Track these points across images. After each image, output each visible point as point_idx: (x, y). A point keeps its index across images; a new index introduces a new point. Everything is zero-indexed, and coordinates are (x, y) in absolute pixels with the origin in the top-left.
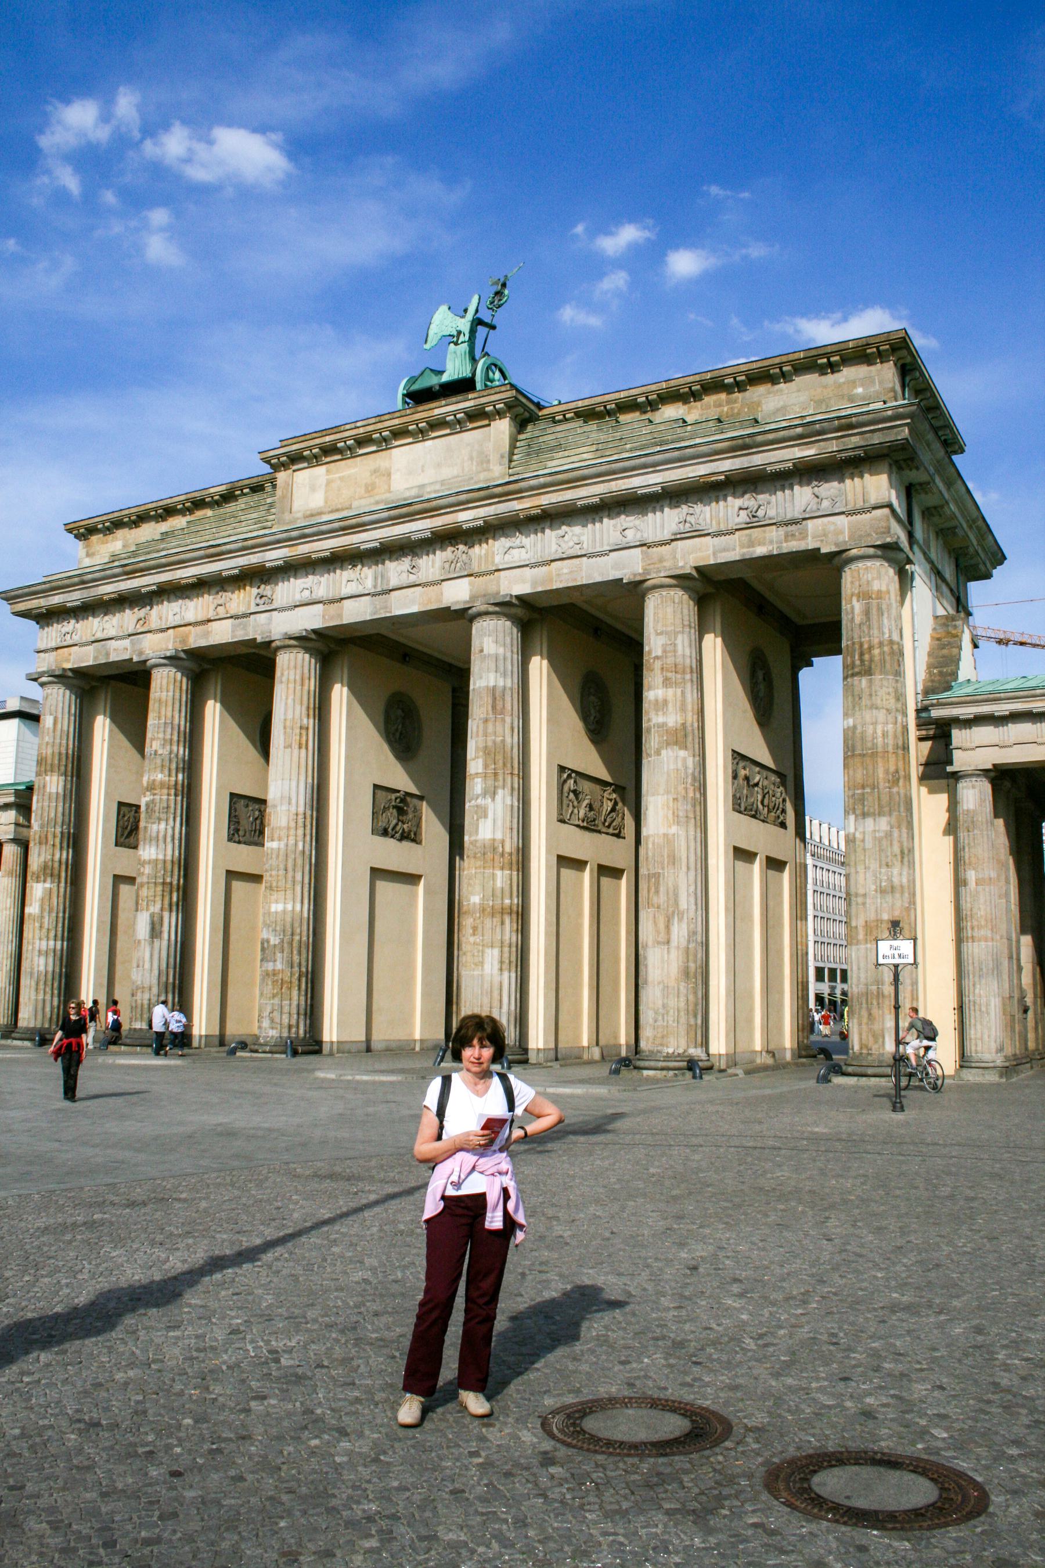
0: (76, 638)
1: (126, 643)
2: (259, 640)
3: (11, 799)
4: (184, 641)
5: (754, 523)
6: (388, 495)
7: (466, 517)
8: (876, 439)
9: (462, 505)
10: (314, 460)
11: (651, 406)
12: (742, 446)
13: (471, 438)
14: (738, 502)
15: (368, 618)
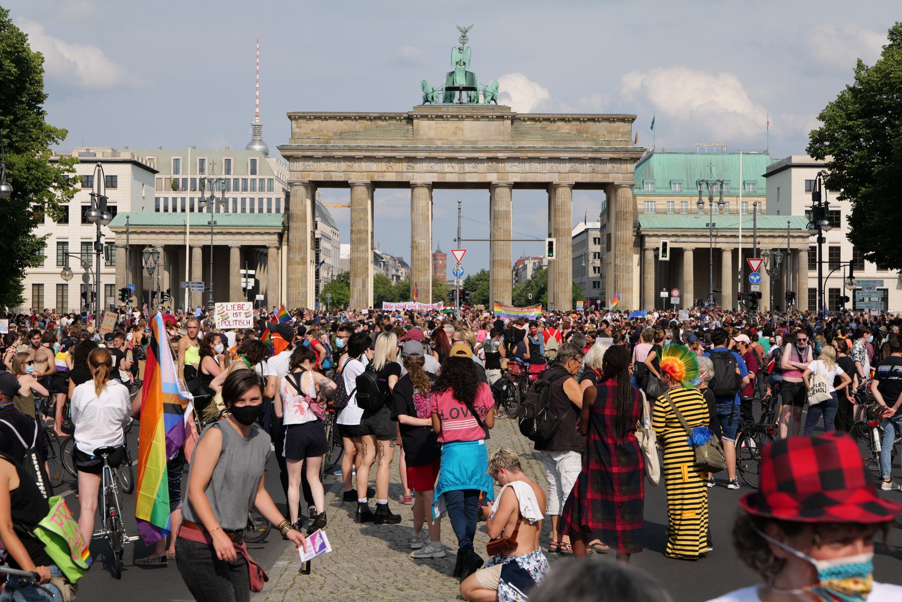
0: (312, 168)
1: (342, 174)
2: (411, 182)
3: (280, 231)
4: (372, 177)
5: (594, 171)
6: (462, 138)
7: (500, 155)
8: (634, 156)
9: (501, 151)
10: (432, 119)
11: (554, 121)
12: (596, 151)
13: (497, 123)
14: (589, 165)
15: (457, 181)
